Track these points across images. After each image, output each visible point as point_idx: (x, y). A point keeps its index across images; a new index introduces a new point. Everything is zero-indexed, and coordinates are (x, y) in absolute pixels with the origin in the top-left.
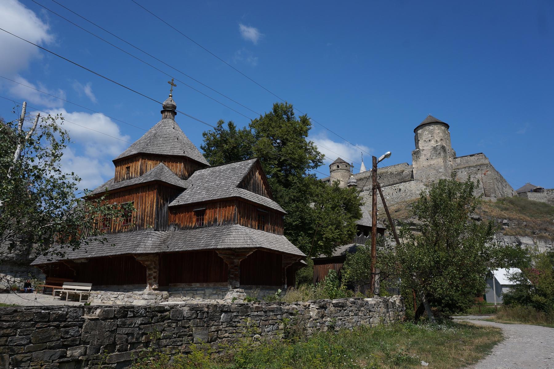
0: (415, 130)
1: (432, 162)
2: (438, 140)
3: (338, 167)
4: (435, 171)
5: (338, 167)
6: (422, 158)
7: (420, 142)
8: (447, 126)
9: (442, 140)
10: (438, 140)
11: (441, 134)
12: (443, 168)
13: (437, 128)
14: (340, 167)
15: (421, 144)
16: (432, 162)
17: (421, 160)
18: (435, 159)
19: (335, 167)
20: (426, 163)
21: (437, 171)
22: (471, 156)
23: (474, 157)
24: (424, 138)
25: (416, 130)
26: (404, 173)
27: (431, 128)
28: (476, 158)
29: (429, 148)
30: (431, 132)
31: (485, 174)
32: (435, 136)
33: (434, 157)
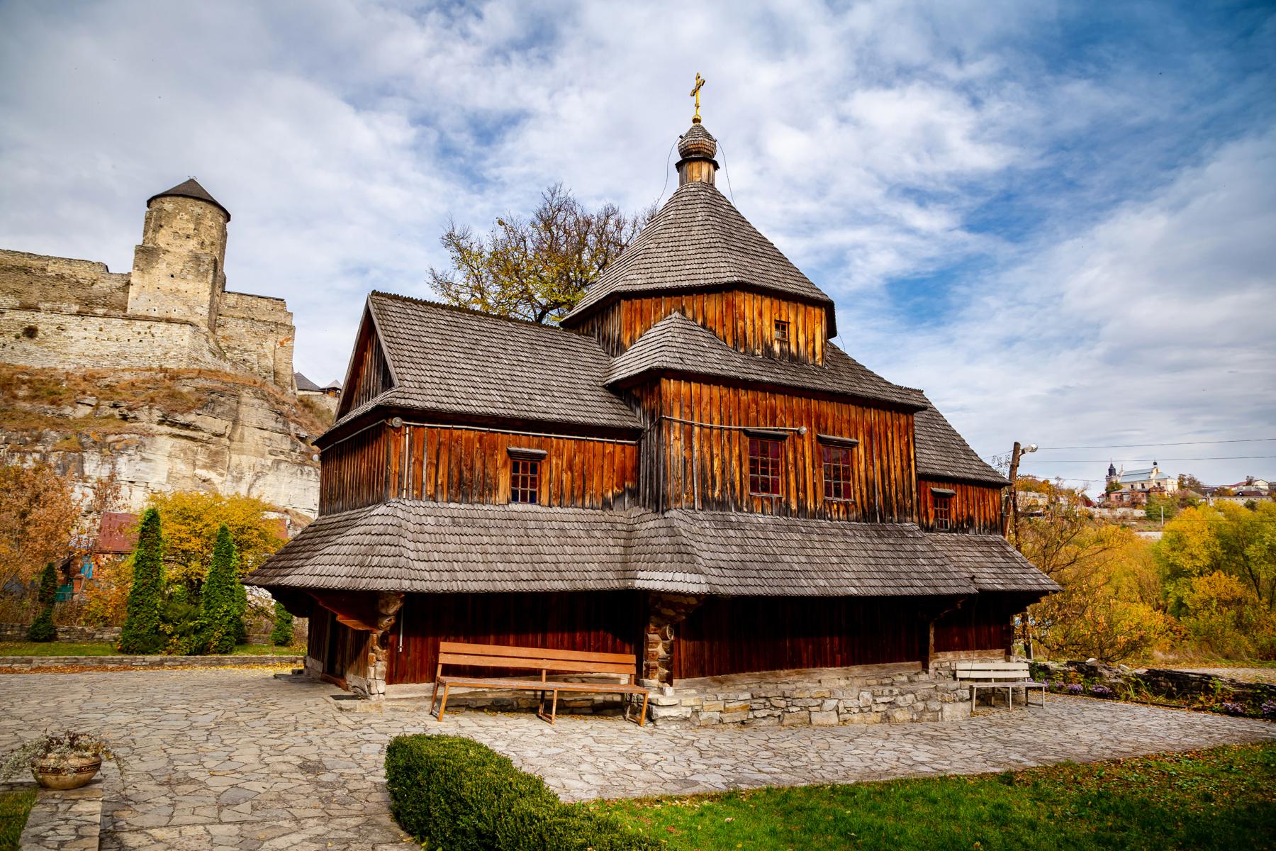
1: (183, 286)
2: (207, 242)
4: (185, 308)
6: (161, 269)
7: (162, 231)
8: (228, 217)
9: (212, 244)
12: (206, 306)
13: (209, 216)
21: (191, 308)
23: (265, 302)
26: (95, 286)
27: (198, 210)
30: (198, 221)
31: (282, 344)
32: (202, 231)
33: (190, 277)
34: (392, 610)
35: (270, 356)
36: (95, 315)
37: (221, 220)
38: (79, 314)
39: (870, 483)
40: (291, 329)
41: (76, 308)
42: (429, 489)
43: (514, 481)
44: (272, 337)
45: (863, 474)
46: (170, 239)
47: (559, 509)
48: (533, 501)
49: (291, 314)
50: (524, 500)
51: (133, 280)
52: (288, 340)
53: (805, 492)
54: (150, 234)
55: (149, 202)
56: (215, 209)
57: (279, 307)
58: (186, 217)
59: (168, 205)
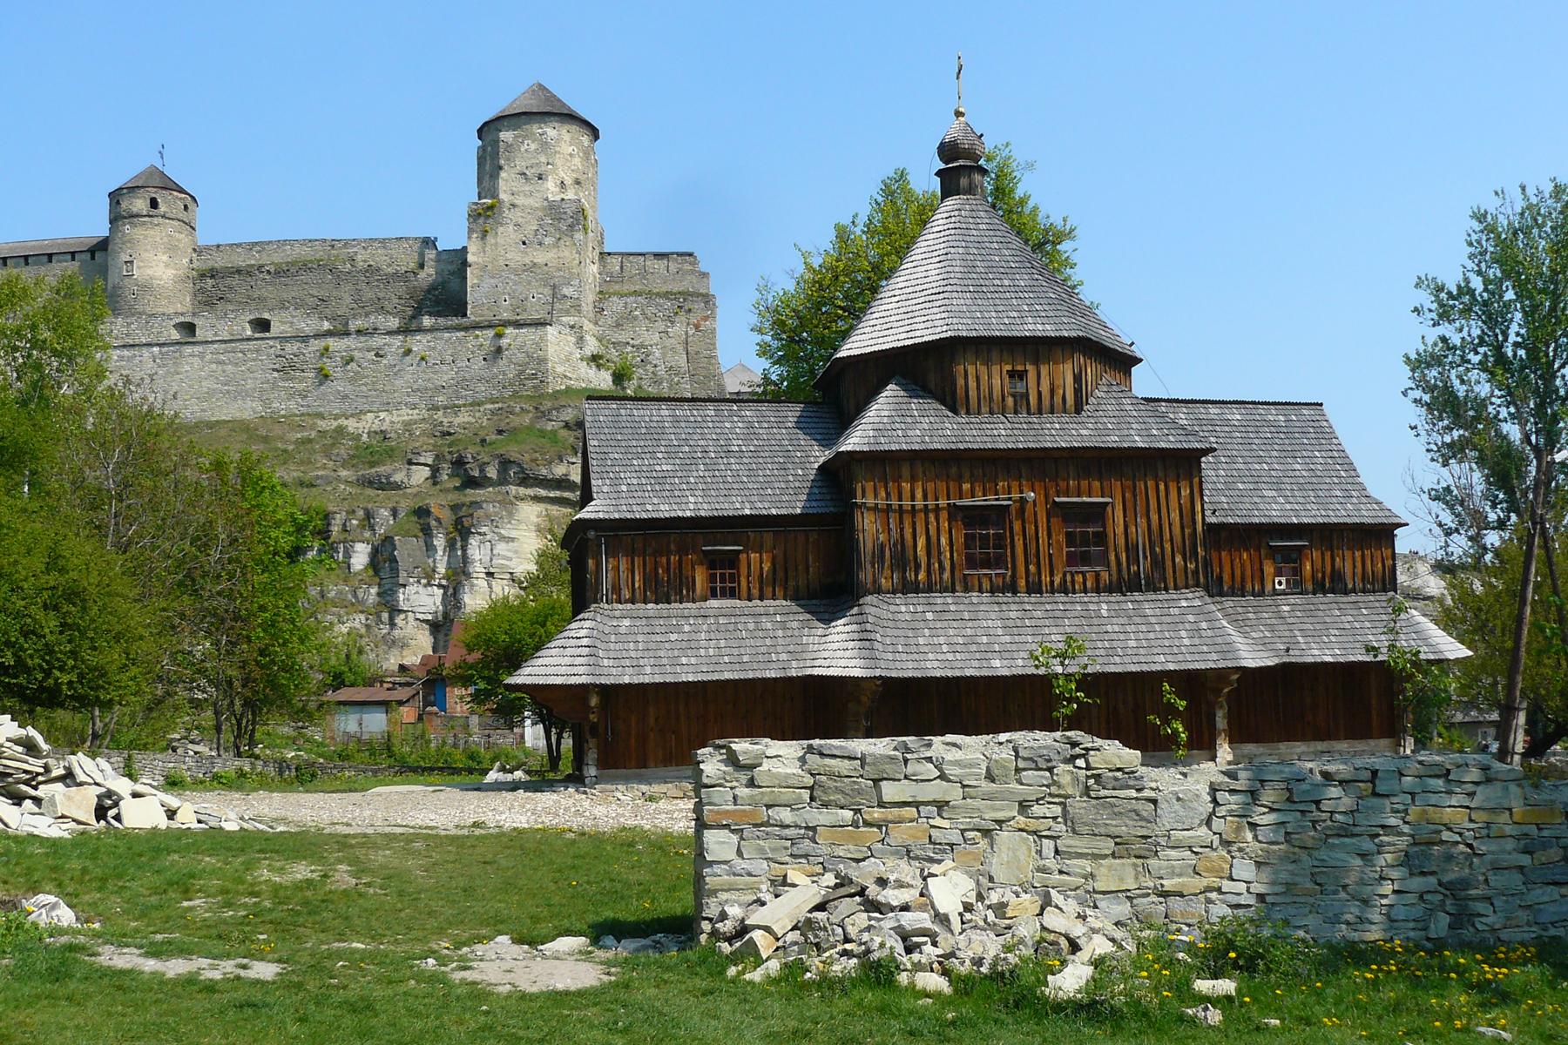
0: (486, 124)
2: (568, 181)
3: (154, 204)
5: (154, 204)
6: (506, 235)
7: (503, 174)
8: (595, 133)
9: (578, 182)
10: (568, 181)
11: (577, 161)
13: (567, 137)
14: (162, 208)
15: (507, 183)
16: (540, 257)
17: (500, 240)
18: (556, 245)
19: (140, 204)
20: (516, 257)
22: (659, 256)
24: (520, 164)
25: (488, 130)
28: (673, 267)
29: (534, 202)
31: (697, 327)
32: (559, 161)
33: (548, 241)
34: (594, 701)
35: (680, 348)
36: (420, 330)
37: (586, 140)
38: (398, 332)
39: (1132, 549)
40: (707, 299)
41: (394, 323)
42: (626, 594)
43: (712, 579)
44: (682, 317)
45: (1121, 541)
46: (519, 184)
47: (758, 602)
48: (732, 594)
49: (705, 275)
50: (724, 595)
51: (470, 258)
52: (706, 318)
53: (1038, 565)
54: (486, 184)
55: (480, 131)
56: (574, 128)
57: (687, 267)
58: (533, 147)
59: (506, 136)
